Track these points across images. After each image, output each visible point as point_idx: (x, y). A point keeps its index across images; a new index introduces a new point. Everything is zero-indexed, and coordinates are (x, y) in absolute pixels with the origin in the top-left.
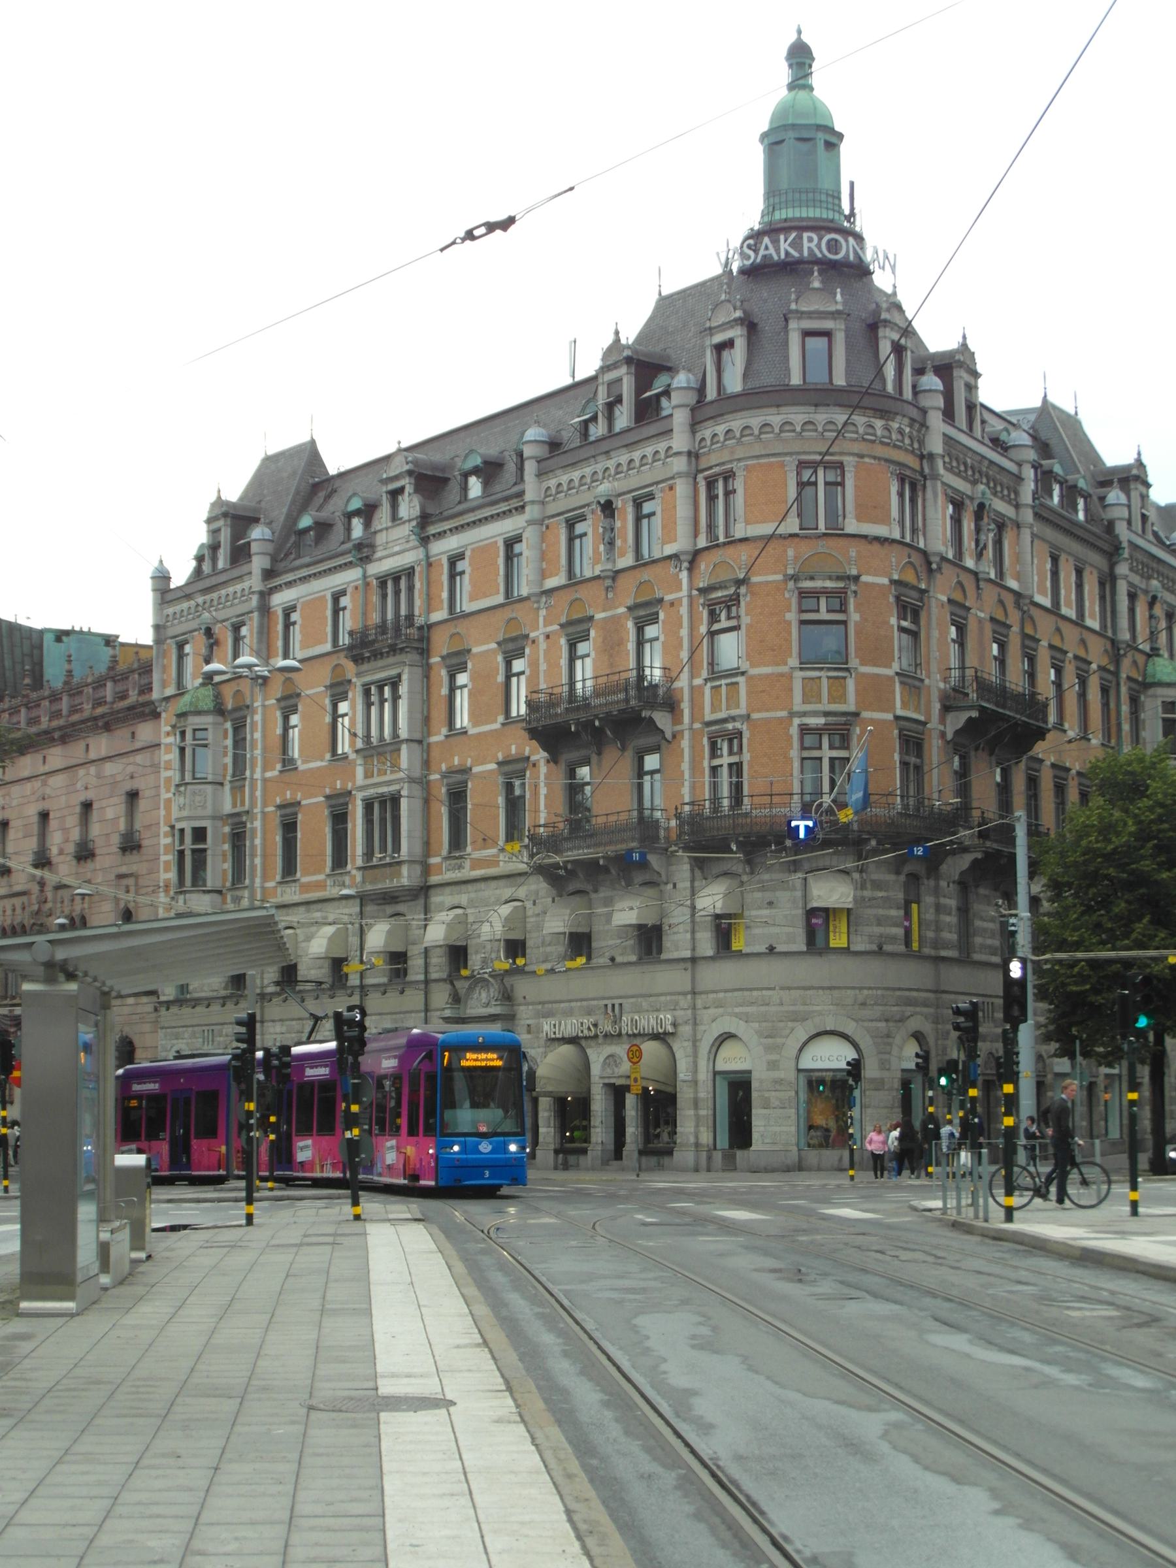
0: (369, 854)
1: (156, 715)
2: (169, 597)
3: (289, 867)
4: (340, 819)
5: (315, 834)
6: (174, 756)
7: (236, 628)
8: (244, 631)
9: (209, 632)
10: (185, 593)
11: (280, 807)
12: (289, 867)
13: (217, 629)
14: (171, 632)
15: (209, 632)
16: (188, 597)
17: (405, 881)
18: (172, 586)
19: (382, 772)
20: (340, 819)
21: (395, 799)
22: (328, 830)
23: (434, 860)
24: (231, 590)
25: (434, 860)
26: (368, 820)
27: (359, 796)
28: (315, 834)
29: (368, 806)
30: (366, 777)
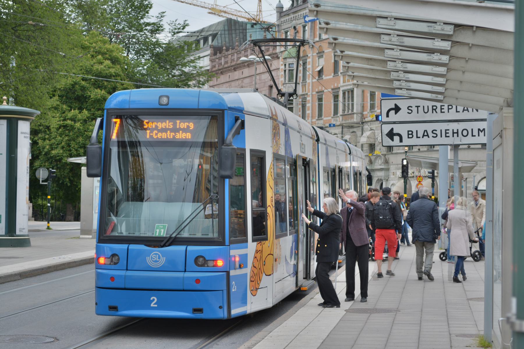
0: (344, 110)
1: (278, 58)
2: (282, 14)
3: (320, 115)
4: (336, 97)
5: (328, 102)
6: (283, 73)
7: (304, 27)
8: (306, 27)
9: (295, 28)
10: (287, 13)
11: (317, 92)
12: (320, 115)
13: (297, 27)
14: (283, 27)
15: (295, 28)
16: (288, 15)
17: (355, 120)
18: (284, 10)
19: (348, 81)
20: (336, 97)
21: (352, 91)
22: (332, 101)
23: (365, 113)
24: (302, 13)
25: (365, 113)
26: (344, 98)
27: (341, 89)
28: (328, 102)
29: (344, 94)
30: (344, 82)
